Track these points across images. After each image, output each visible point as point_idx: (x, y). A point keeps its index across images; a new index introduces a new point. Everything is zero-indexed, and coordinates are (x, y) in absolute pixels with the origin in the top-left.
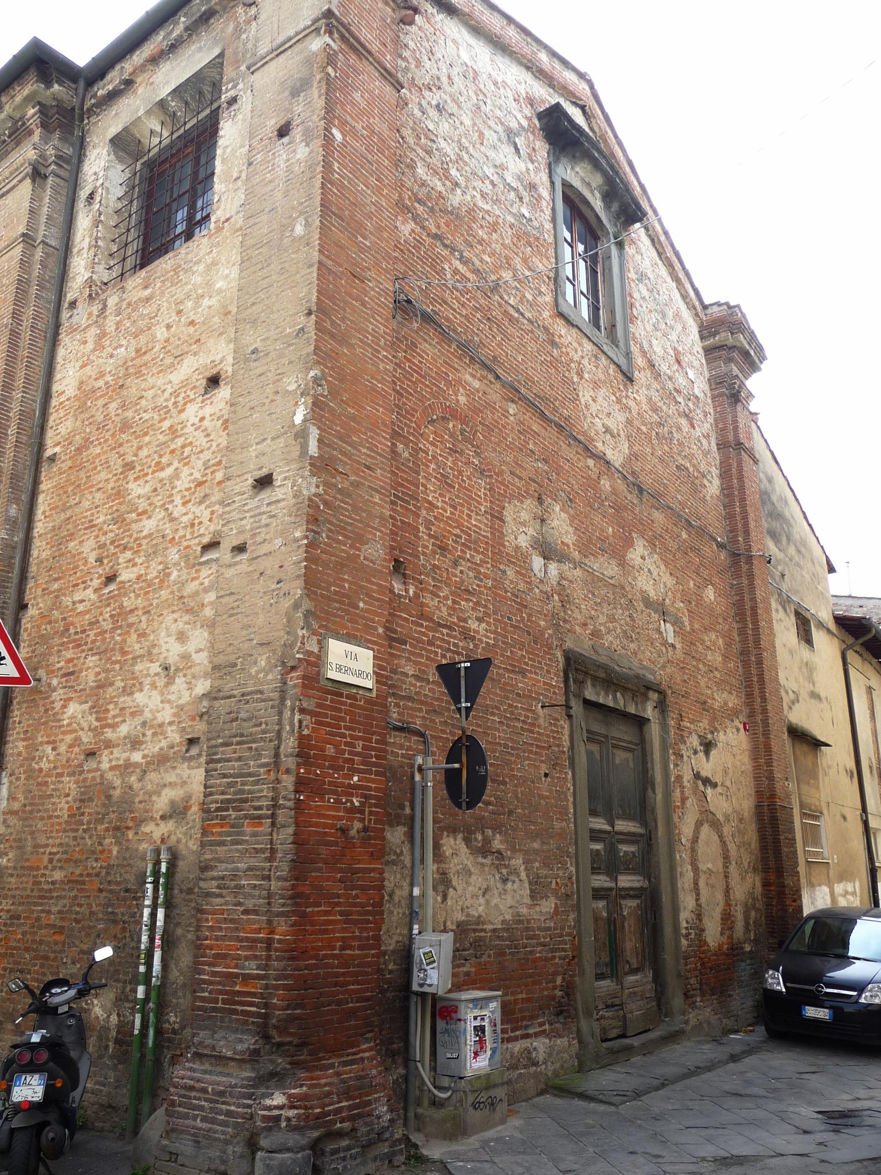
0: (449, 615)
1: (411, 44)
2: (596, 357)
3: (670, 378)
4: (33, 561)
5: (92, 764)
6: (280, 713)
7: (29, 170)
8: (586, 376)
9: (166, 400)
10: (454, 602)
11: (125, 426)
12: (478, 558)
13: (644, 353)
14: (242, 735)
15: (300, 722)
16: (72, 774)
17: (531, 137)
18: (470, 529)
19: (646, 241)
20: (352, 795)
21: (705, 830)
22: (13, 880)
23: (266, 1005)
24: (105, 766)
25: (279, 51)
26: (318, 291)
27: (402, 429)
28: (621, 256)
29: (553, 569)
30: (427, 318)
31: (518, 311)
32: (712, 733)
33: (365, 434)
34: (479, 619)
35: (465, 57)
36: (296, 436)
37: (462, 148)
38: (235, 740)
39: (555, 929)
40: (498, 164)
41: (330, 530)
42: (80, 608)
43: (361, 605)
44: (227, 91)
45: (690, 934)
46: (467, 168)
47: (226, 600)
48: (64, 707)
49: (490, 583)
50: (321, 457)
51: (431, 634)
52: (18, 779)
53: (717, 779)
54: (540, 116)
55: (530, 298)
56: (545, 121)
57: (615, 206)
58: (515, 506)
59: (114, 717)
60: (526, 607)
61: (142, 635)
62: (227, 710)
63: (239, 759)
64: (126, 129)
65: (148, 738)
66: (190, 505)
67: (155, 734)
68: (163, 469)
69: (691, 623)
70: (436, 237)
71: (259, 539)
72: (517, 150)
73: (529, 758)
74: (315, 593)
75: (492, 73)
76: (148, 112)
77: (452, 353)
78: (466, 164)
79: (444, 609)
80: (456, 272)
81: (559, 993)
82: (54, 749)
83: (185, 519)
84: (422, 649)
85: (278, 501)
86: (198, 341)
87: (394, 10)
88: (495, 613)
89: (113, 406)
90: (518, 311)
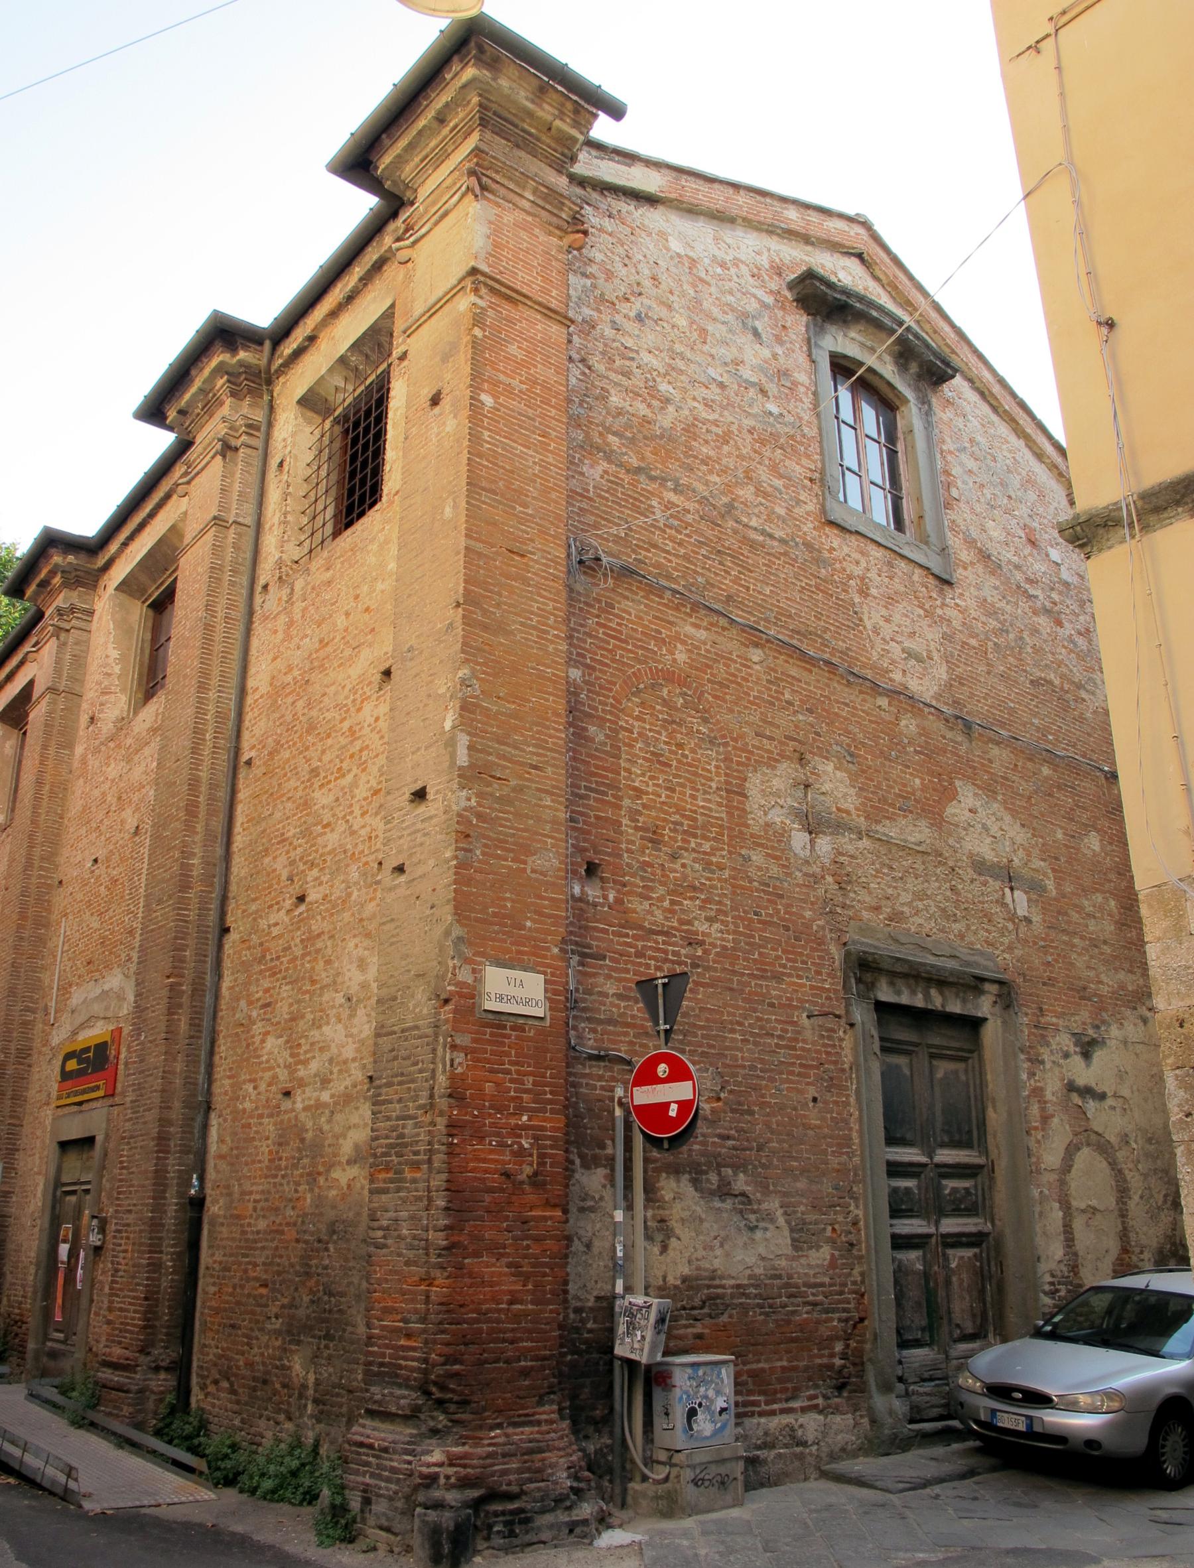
0: (666, 919)
1: (599, 257)
2: (890, 565)
3: (1018, 567)
4: (233, 879)
5: (287, 1104)
6: (434, 1050)
7: (219, 446)
8: (873, 591)
9: (347, 698)
10: (672, 902)
11: (311, 728)
12: (707, 846)
13: (970, 543)
14: (402, 1074)
15: (452, 1061)
16: (271, 1116)
17: (780, 314)
18: (695, 812)
19: (973, 397)
20: (520, 1136)
21: (1084, 1156)
22: (224, 1229)
23: (426, 1361)
24: (299, 1106)
25: (432, 312)
26: (466, 581)
27: (596, 709)
28: (928, 425)
29: (824, 844)
30: (626, 573)
31: (763, 532)
32: (1097, 1027)
33: (530, 730)
34: (710, 920)
35: (675, 245)
36: (446, 745)
37: (673, 354)
38: (396, 1080)
39: (831, 1285)
40: (728, 360)
41: (485, 846)
42: (275, 931)
43: (528, 924)
44: (398, 345)
45: (1057, 1291)
46: (683, 378)
47: (386, 928)
48: (263, 1041)
49: (726, 874)
50: (472, 766)
51: (640, 944)
52: (225, 1120)
53: (1106, 1087)
54: (791, 286)
55: (781, 511)
56: (795, 291)
57: (914, 368)
58: (764, 774)
59: (306, 1052)
60: (781, 896)
61: (328, 962)
62: (390, 1047)
63: (400, 1101)
64: (310, 390)
65: (335, 1076)
66: (367, 817)
67: (340, 1071)
68: (344, 776)
69: (1058, 886)
70: (638, 470)
71: (415, 860)
72: (756, 333)
73: (788, 1081)
74: (468, 918)
75: (717, 252)
76: (331, 370)
77: (665, 605)
78: (681, 372)
79: (658, 913)
80: (669, 505)
81: (838, 1362)
82: (255, 1088)
83: (363, 832)
84: (626, 962)
85: (431, 818)
86: (373, 630)
87: (561, 238)
88: (733, 909)
89: (300, 704)
90: (763, 532)
